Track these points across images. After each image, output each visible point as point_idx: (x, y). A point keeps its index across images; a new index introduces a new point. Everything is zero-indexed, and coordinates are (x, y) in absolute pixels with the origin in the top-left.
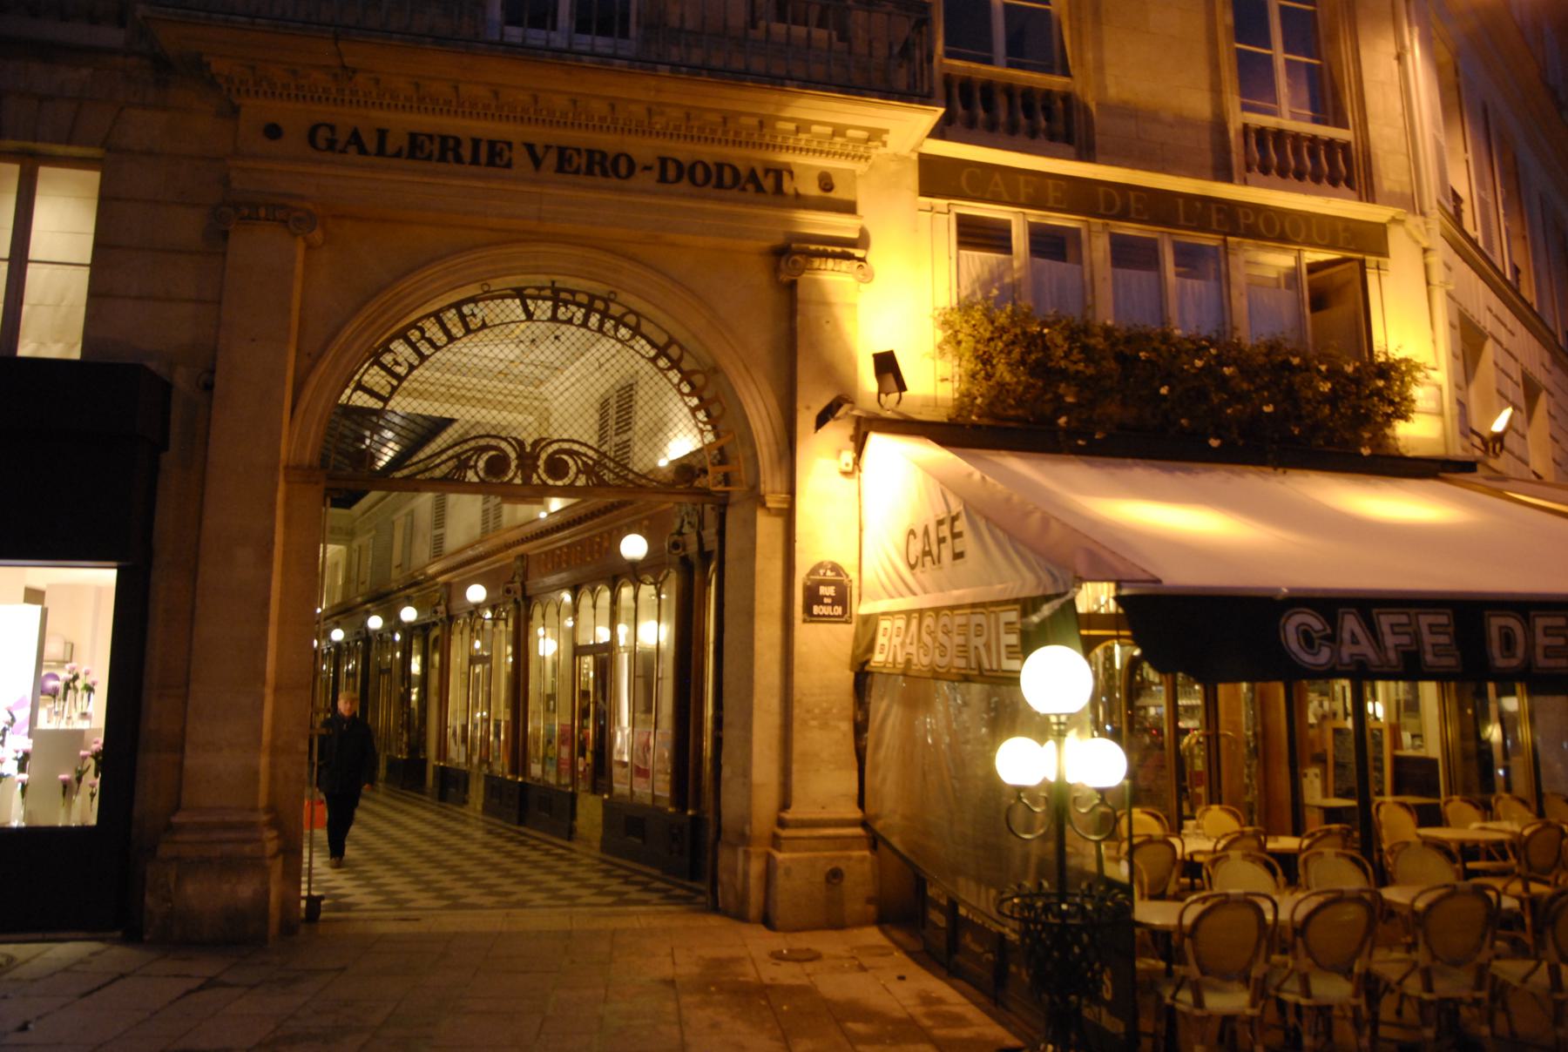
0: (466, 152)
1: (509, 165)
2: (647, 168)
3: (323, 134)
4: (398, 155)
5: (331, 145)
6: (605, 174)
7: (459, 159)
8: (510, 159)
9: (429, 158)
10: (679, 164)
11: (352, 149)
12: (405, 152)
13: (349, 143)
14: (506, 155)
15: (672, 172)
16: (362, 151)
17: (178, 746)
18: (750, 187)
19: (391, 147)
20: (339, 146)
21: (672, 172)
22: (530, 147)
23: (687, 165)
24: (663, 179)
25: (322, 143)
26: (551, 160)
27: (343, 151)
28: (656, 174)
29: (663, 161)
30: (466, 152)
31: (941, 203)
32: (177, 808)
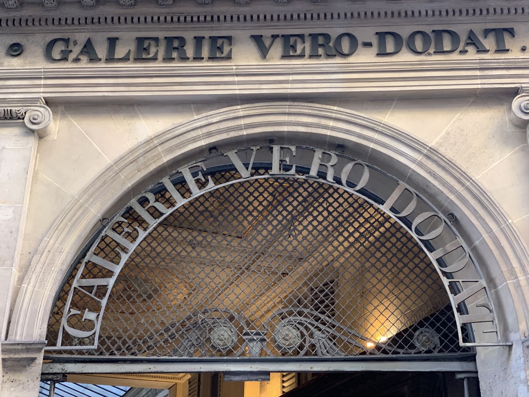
1: (229, 58)
2: (368, 45)
4: (125, 59)
7: (184, 59)
8: (231, 51)
14: (226, 49)
15: (390, 47)
19: (120, 52)
20: (72, 56)
21: (390, 47)
25: (56, 55)
27: (77, 60)
28: (375, 50)
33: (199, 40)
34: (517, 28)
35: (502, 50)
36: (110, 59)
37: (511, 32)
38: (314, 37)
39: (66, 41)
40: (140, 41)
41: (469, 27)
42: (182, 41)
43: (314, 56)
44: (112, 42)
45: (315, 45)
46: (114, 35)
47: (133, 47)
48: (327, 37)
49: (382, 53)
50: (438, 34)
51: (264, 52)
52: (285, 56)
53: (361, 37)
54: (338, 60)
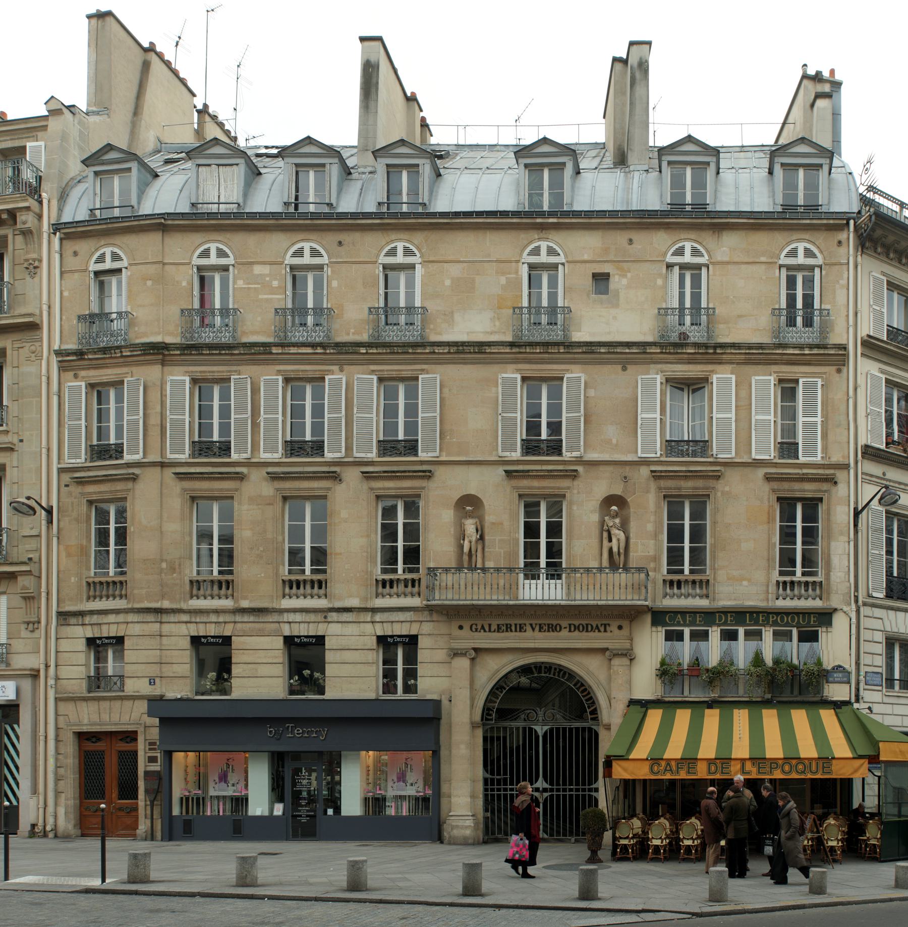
0: (513, 628)
1: (525, 631)
3: (474, 627)
4: (494, 631)
6: (553, 631)
7: (511, 631)
9: (503, 632)
10: (575, 625)
11: (482, 631)
15: (573, 629)
16: (485, 631)
17: (450, 797)
18: (597, 631)
19: (492, 629)
21: (573, 629)
22: (531, 625)
23: (577, 625)
24: (570, 631)
25: (474, 630)
26: (537, 628)
28: (568, 629)
30: (513, 628)
31: (660, 628)
32: (450, 812)
33: (516, 625)
34: (610, 623)
35: (605, 631)
36: (490, 631)
37: (609, 625)
38: (548, 625)
39: (476, 625)
40: (498, 625)
41: (597, 622)
42: (511, 625)
43: (549, 631)
44: (490, 625)
45: (549, 628)
46: (490, 622)
47: (496, 627)
48: (552, 625)
49: (570, 631)
50: (587, 625)
51: (533, 629)
52: (540, 631)
53: (563, 626)
54: (555, 634)
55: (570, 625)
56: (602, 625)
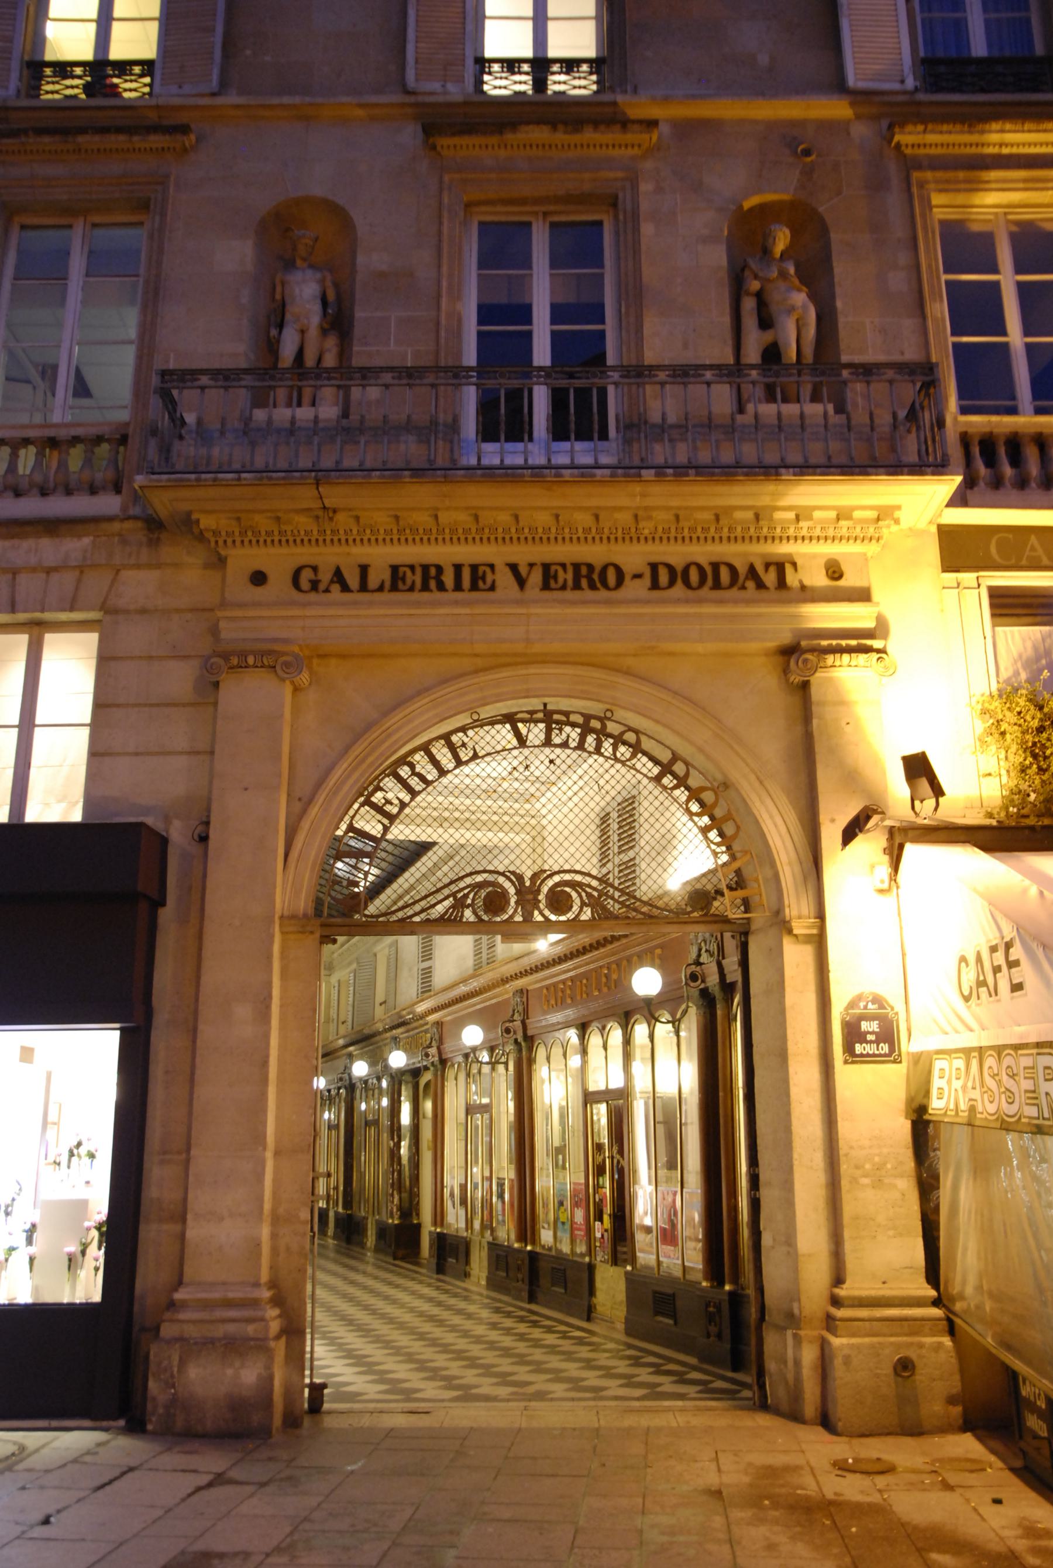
0: (448, 579)
4: (381, 589)
5: (315, 585)
6: (592, 587)
7: (441, 587)
8: (494, 582)
10: (671, 568)
12: (387, 585)
13: (332, 582)
15: (664, 577)
18: (750, 584)
19: (373, 582)
21: (664, 577)
23: (679, 569)
27: (327, 591)
28: (647, 581)
29: (654, 567)
30: (448, 579)
47: (387, 576)
55: (654, 567)
56: (767, 566)
